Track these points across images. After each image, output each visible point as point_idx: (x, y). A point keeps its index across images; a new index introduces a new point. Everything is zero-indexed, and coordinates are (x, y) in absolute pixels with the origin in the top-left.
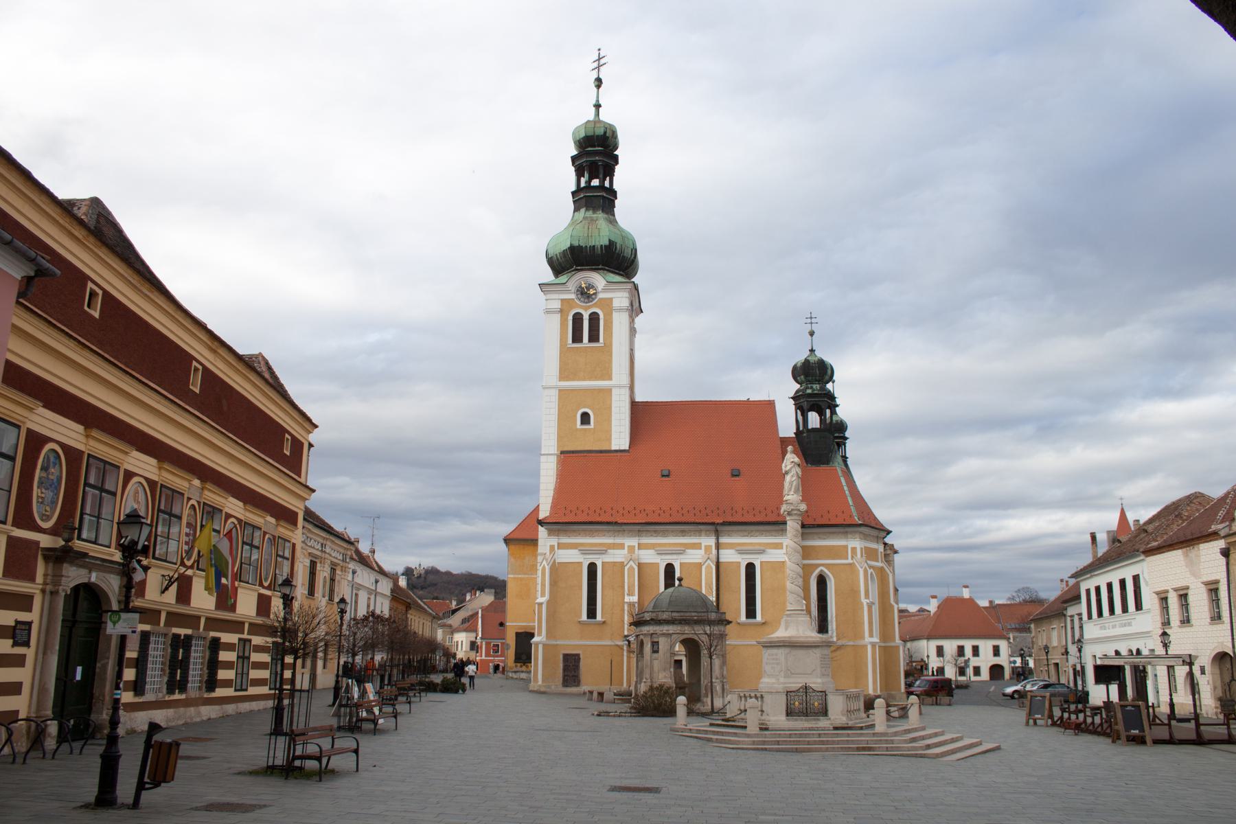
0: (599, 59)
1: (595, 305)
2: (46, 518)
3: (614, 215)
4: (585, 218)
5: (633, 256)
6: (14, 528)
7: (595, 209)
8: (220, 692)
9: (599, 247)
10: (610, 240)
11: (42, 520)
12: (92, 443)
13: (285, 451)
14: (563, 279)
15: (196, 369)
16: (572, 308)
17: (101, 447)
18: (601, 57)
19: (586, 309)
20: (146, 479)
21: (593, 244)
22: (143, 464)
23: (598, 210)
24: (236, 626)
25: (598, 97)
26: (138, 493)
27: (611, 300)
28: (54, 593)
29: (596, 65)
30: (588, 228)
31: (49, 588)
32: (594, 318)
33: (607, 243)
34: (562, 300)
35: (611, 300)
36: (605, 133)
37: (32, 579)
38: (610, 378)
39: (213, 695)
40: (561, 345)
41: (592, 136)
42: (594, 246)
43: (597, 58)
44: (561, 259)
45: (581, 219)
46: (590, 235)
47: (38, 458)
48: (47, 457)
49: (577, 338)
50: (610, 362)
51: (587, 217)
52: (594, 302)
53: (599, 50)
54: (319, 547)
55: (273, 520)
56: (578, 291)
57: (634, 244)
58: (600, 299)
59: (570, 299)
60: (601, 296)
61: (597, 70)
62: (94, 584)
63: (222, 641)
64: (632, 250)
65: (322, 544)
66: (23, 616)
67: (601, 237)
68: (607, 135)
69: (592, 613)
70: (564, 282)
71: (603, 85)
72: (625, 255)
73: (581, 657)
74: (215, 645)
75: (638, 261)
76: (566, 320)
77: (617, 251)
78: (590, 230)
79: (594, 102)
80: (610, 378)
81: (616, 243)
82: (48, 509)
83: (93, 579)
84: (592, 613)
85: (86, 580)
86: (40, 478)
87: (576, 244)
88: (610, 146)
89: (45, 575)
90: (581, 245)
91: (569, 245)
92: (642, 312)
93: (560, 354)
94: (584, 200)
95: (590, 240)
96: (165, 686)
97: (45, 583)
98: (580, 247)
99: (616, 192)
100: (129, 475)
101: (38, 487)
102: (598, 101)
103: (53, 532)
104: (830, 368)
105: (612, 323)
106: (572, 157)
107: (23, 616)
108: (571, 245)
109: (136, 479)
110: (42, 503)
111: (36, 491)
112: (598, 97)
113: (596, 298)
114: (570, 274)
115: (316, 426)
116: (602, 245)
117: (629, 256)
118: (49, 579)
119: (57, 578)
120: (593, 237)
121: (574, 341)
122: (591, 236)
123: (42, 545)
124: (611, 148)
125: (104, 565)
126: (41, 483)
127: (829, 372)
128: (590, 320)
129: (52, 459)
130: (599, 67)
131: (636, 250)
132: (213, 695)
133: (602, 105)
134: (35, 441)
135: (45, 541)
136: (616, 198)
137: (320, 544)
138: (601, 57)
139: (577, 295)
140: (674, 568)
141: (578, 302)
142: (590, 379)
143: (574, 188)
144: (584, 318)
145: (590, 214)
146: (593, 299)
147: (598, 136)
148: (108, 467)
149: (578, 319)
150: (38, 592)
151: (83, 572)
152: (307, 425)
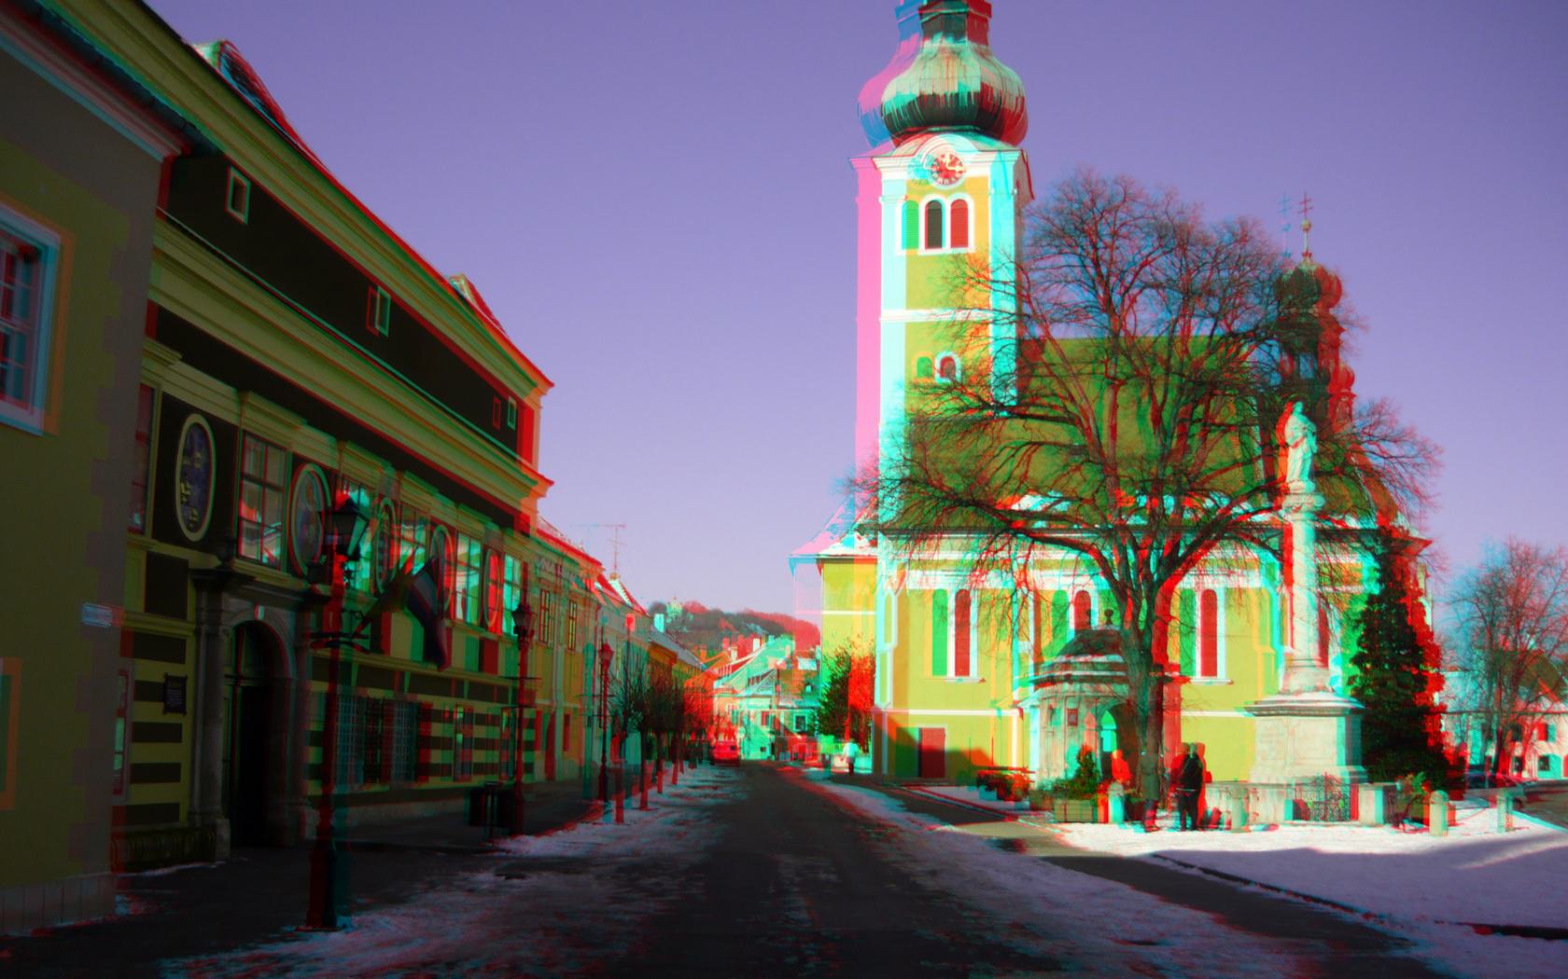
1: (962, 189)
2: (195, 528)
5: (1019, 108)
6: (156, 542)
7: (958, 36)
8: (435, 783)
11: (189, 529)
12: (248, 413)
13: (509, 424)
15: (383, 299)
16: (924, 193)
17: (259, 417)
19: (947, 194)
20: (324, 468)
21: (956, 91)
22: (314, 444)
24: (451, 687)
26: (312, 488)
28: (213, 636)
31: (204, 628)
32: (960, 210)
33: (977, 88)
37: (181, 615)
39: (424, 786)
42: (957, 95)
44: (905, 115)
45: (935, 51)
46: (950, 76)
47: (178, 436)
48: (190, 437)
49: (934, 240)
52: (960, 182)
54: (552, 569)
55: (495, 528)
58: (972, 180)
62: (260, 623)
63: (434, 708)
65: (556, 565)
66: (175, 670)
69: (962, 667)
72: (1006, 106)
73: (947, 733)
74: (426, 714)
75: (1026, 117)
78: (950, 68)
82: (195, 512)
83: (260, 616)
84: (962, 667)
85: (247, 617)
86: (183, 466)
87: (929, 91)
89: (198, 609)
91: (918, 95)
96: (362, 773)
97: (199, 622)
98: (935, 96)
100: (298, 461)
101: (181, 481)
103: (203, 546)
104: (1335, 282)
107: (175, 670)
109: (309, 468)
110: (187, 504)
111: (180, 487)
114: (919, 141)
115: (551, 385)
118: (204, 615)
119: (215, 612)
122: (953, 78)
123: (191, 566)
125: (272, 595)
126: (184, 474)
127: (1335, 286)
128: (953, 212)
129: (196, 438)
132: (424, 786)
134: (175, 411)
135: (194, 559)
136: (990, 15)
137: (553, 565)
140: (1089, 598)
141: (934, 184)
145: (948, 43)
146: (957, 179)
148: (271, 449)
149: (934, 211)
150: (191, 634)
151: (247, 604)
152: (536, 379)
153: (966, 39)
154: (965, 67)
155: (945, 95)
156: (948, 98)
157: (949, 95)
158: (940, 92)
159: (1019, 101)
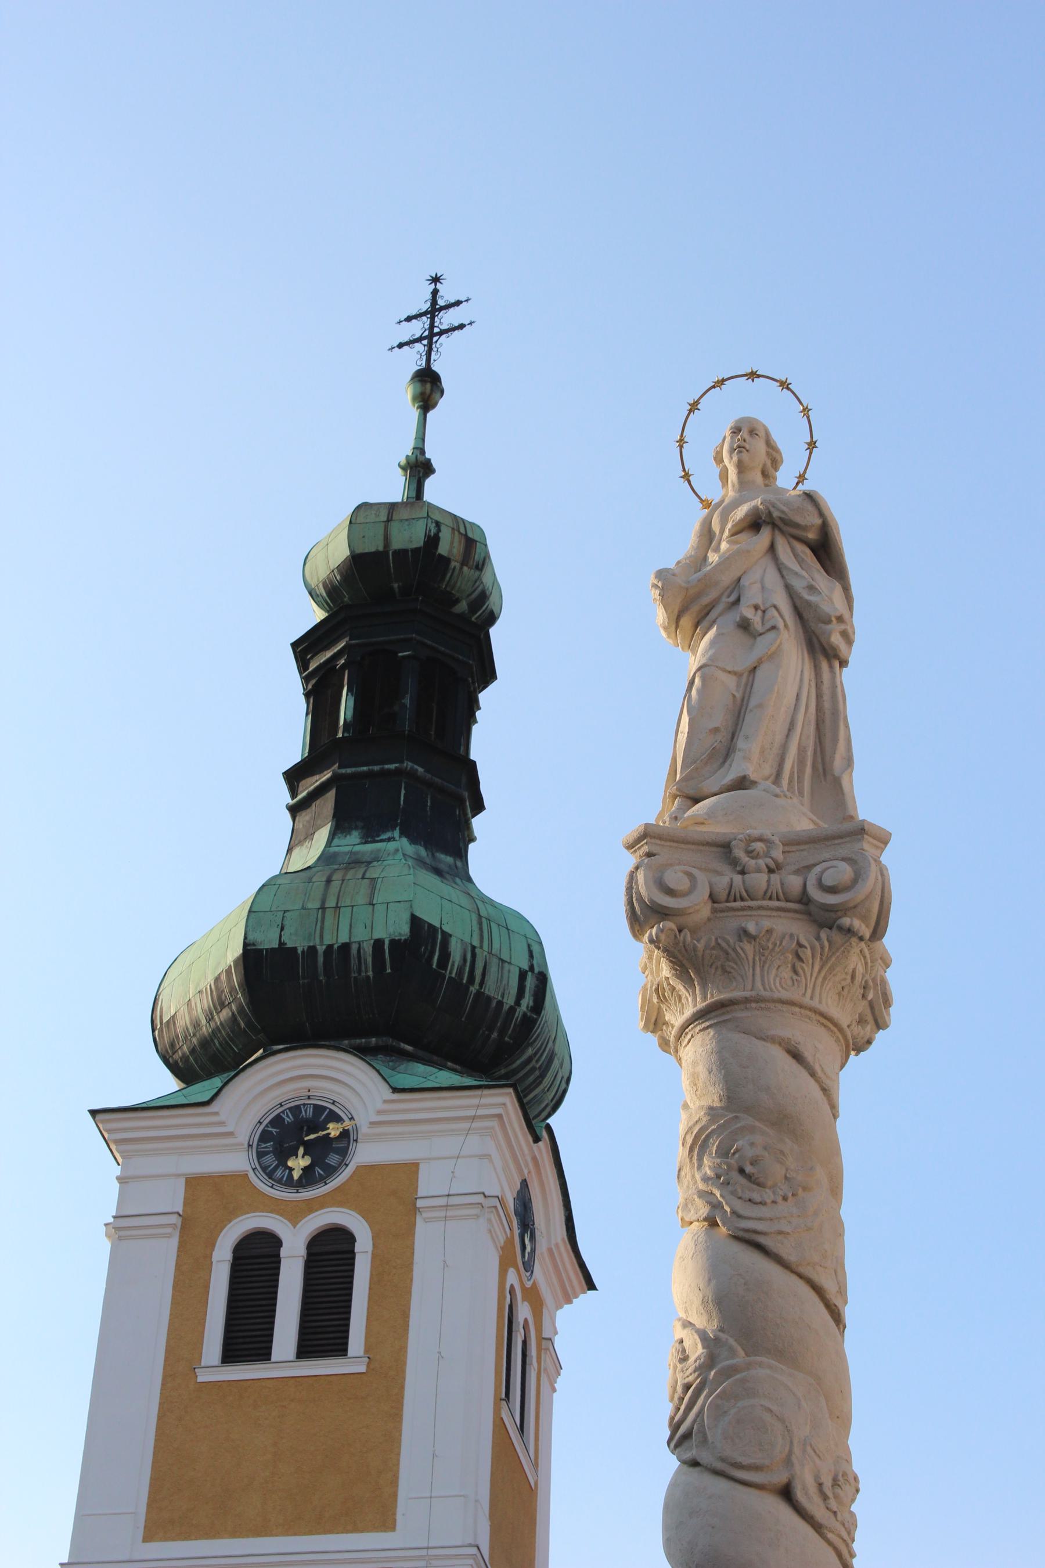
0: (434, 310)
3: (469, 880)
4: (326, 858)
5: (527, 1001)
9: (368, 948)
10: (416, 922)
14: (202, 1090)
16: (232, 1213)
18: (441, 302)
19: (295, 1214)
21: (343, 938)
23: (387, 824)
25: (421, 437)
27: (411, 1169)
29: (418, 328)
30: (329, 881)
33: (404, 930)
34: (194, 1183)
35: (411, 1169)
36: (432, 541)
38: (386, 1521)
40: (168, 1376)
41: (376, 553)
42: (345, 947)
43: (427, 306)
46: (331, 903)
50: (392, 1441)
51: (335, 855)
53: (436, 280)
56: (265, 1137)
57: (534, 949)
59: (224, 1177)
60: (364, 1154)
61: (420, 347)
64: (523, 975)
67: (380, 909)
68: (443, 549)
70: (206, 1098)
71: (442, 403)
72: (491, 989)
76: (205, 1264)
77: (452, 971)
78: (335, 885)
79: (405, 450)
80: (386, 1521)
81: (446, 936)
87: (269, 940)
88: (457, 601)
90: (289, 945)
92: (591, 1286)
93: (161, 1417)
94: (331, 795)
95: (328, 923)
98: (284, 953)
99: (475, 762)
102: (420, 450)
105: (409, 1266)
106: (295, 645)
108: (245, 945)
112: (421, 437)
113: (343, 1164)
116: (378, 944)
117: (509, 1001)
120: (345, 913)
121: (231, 1354)
122: (337, 907)
124: (463, 607)
130: (430, 337)
131: (543, 979)
133: (435, 464)
136: (478, 806)
138: (441, 302)
139: (260, 1155)
142: (291, 1528)
143: (295, 752)
144: (284, 1252)
145: (351, 842)
147: (401, 554)
153: (396, 833)
154: (373, 881)
155: (312, 950)
156: (321, 959)
157: (321, 949)
158: (297, 941)
159: (530, 982)
